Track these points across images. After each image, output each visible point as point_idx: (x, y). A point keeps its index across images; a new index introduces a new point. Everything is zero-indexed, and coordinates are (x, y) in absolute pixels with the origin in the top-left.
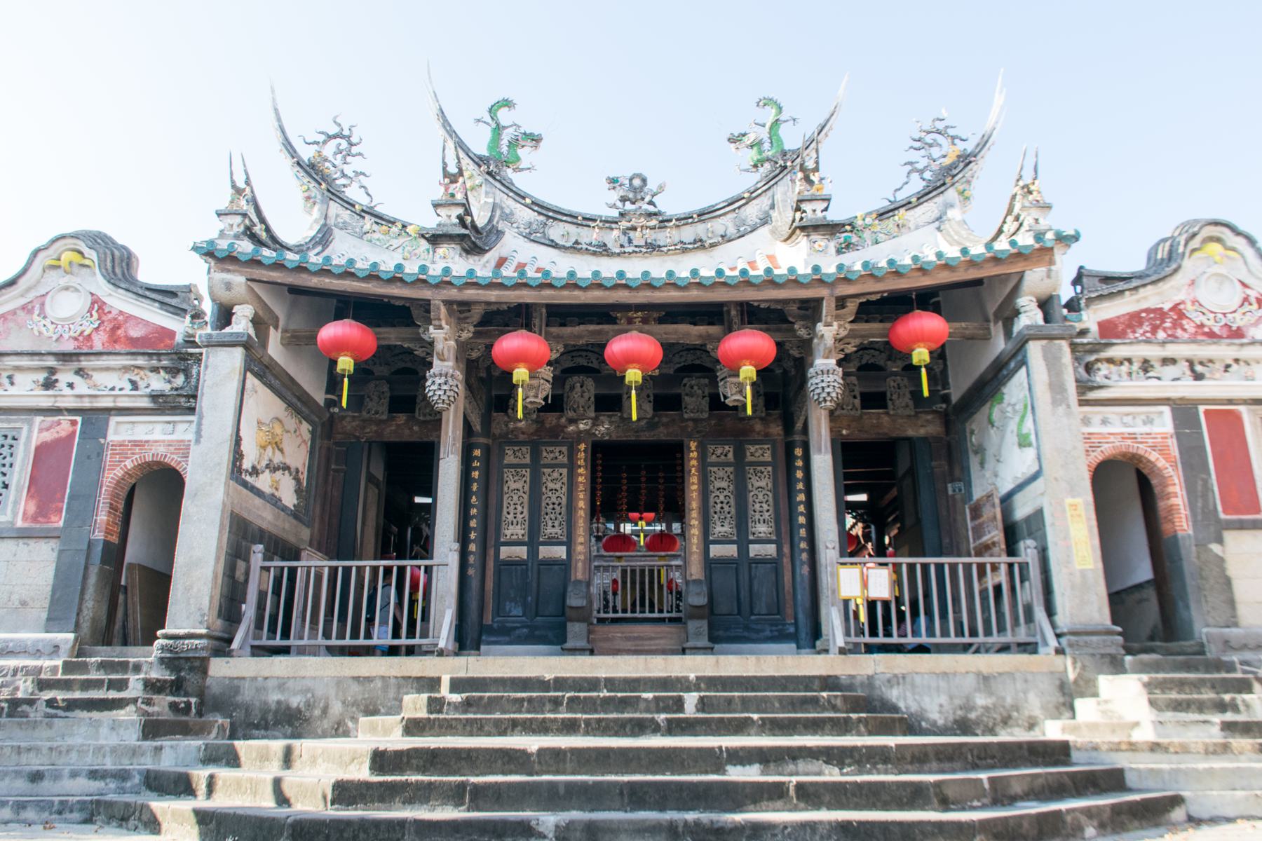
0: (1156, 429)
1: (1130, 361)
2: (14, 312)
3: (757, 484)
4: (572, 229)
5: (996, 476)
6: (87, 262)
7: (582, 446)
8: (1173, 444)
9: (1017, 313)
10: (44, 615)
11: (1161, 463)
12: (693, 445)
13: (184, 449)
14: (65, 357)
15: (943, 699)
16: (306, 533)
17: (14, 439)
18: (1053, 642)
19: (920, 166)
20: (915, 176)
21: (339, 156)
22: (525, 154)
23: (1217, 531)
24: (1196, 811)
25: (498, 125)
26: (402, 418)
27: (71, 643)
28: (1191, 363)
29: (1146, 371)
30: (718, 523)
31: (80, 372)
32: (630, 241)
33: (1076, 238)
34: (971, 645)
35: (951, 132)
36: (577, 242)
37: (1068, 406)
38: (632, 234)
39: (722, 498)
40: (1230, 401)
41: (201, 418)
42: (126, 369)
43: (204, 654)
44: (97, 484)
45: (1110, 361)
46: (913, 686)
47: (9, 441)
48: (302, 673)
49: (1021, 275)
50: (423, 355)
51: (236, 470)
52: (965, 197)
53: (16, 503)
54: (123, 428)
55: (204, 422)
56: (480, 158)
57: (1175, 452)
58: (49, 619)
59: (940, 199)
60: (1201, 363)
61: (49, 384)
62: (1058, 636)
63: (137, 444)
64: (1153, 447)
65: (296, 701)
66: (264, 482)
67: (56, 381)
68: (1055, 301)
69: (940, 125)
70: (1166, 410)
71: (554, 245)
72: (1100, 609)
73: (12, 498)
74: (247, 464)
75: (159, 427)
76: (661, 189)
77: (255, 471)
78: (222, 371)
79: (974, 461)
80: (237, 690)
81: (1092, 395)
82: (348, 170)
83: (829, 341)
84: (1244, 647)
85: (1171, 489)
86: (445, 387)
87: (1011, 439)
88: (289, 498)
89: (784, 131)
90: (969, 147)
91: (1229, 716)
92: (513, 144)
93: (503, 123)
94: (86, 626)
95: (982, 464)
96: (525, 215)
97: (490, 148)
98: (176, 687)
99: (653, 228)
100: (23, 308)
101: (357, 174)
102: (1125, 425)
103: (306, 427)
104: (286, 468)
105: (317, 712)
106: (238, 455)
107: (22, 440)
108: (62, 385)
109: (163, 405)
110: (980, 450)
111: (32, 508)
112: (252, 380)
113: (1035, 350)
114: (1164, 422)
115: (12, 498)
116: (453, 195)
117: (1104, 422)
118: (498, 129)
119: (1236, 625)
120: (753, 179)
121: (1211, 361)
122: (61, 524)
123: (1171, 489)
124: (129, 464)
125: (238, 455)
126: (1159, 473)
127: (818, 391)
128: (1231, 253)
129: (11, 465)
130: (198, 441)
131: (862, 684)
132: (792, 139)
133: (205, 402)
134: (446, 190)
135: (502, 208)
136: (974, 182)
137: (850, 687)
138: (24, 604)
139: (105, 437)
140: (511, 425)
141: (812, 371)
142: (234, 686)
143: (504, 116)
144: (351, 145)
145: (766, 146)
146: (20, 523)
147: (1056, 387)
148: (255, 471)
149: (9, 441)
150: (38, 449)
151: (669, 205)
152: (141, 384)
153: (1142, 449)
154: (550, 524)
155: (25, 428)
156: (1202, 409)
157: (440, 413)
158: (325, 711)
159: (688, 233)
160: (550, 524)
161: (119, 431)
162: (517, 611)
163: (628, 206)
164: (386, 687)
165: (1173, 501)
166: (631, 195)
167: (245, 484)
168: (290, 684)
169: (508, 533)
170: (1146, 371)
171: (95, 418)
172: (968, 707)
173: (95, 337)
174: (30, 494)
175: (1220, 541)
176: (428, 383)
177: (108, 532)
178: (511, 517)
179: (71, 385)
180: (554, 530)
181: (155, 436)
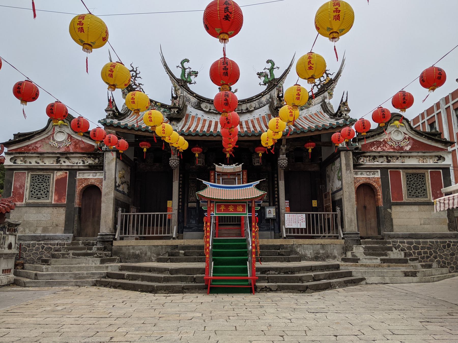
0: (376, 176)
2: (44, 139)
3: (264, 185)
4: (209, 105)
6: (66, 124)
8: (380, 180)
10: (63, 229)
11: (376, 186)
13: (101, 181)
14: (62, 154)
15: (311, 251)
16: (130, 200)
18: (342, 236)
19: (317, 84)
20: (315, 87)
21: (133, 78)
22: (192, 78)
23: (391, 205)
24: (368, 281)
25: (184, 67)
26: (158, 164)
27: (72, 237)
28: (387, 157)
31: (67, 158)
34: (320, 236)
35: (327, 72)
36: (210, 110)
40: (397, 168)
41: (105, 173)
42: (80, 157)
43: (112, 240)
44: (74, 191)
45: (365, 156)
46: (304, 248)
47: (47, 178)
48: (139, 244)
51: (116, 186)
52: (331, 95)
53: (52, 197)
54: (81, 175)
56: (178, 79)
57: (380, 183)
58: (65, 230)
59: (322, 95)
60: (390, 157)
61: (58, 162)
62: (343, 234)
63: (85, 179)
64: (374, 182)
65: (138, 252)
66: (120, 189)
67: (60, 160)
70: (379, 171)
71: (202, 110)
72: (355, 227)
74: (117, 184)
75: (91, 174)
77: (119, 186)
78: (110, 159)
79: (327, 179)
80: (121, 249)
82: (137, 82)
83: (284, 151)
84: (394, 237)
85: (378, 193)
87: (336, 176)
88: (126, 191)
89: (275, 72)
90: (332, 77)
91: (382, 257)
92: (190, 74)
93: (186, 67)
94: (75, 232)
96: (194, 100)
97: (181, 76)
98: (105, 249)
100: (47, 137)
101: (140, 84)
102: (367, 175)
103: (129, 168)
104: (125, 182)
105: (143, 255)
106: (116, 182)
107: (52, 178)
108: (62, 162)
109: (91, 168)
110: (329, 177)
111: (56, 198)
112: (118, 159)
113: (343, 154)
114: (378, 175)
115: (50, 195)
116: (175, 104)
117: (361, 174)
118: (184, 69)
119: (393, 231)
120: (264, 88)
122: (66, 202)
123: (378, 193)
124: (84, 185)
125: (116, 182)
128: (402, 124)
130: (105, 180)
131: (290, 247)
132: (277, 74)
134: (173, 102)
135: (186, 97)
136: (334, 90)
137: (287, 248)
138: (57, 225)
139: (76, 177)
140: (191, 167)
142: (120, 248)
143: (186, 65)
144: (137, 74)
145: (269, 77)
146: (53, 202)
147: (347, 165)
148: (119, 186)
149: (47, 178)
150: (56, 181)
152: (86, 162)
155: (52, 175)
156: (389, 170)
157: (173, 170)
158: (146, 254)
161: (80, 176)
162: (194, 222)
164: (162, 248)
165: (379, 197)
167: (117, 190)
168: (136, 247)
169: (191, 199)
171: (73, 171)
172: (318, 253)
173: (70, 147)
174: (55, 194)
175: (391, 208)
176: (170, 162)
177: (79, 205)
178: (191, 194)
179: (64, 162)
181: (91, 177)
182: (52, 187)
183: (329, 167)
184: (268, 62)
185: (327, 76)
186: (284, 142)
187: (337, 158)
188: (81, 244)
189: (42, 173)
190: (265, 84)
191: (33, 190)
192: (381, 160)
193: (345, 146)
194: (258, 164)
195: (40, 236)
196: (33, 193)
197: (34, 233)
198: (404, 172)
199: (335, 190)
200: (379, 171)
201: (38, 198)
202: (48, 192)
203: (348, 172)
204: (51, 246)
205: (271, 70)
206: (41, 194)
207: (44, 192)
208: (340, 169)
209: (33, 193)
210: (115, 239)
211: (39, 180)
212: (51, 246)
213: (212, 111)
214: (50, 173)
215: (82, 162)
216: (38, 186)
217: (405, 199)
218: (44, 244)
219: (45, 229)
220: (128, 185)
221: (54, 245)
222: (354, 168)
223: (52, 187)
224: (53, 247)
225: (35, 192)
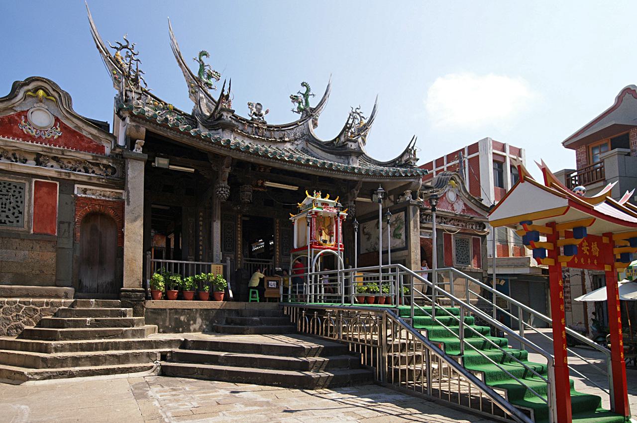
12: (278, 221)
17: (20, 188)
35: (361, 115)
50: (203, 174)
69: (358, 111)
73: (26, 219)
76: (267, 112)
89: (310, 98)
115: (26, 219)
120: (298, 117)
129: (22, 202)
132: (313, 104)
151: (271, 120)
154: (228, 245)
159: (277, 135)
160: (228, 245)
163: (254, 117)
182: (29, 206)
184: (303, 84)
185: (361, 120)
189: (6, 179)
190: (298, 112)
202: (20, 213)
205: (306, 95)
206: (7, 217)
207: (13, 214)
210: (147, 298)
214: (23, 181)
215: (83, 170)
218: (20, 302)
223: (29, 206)
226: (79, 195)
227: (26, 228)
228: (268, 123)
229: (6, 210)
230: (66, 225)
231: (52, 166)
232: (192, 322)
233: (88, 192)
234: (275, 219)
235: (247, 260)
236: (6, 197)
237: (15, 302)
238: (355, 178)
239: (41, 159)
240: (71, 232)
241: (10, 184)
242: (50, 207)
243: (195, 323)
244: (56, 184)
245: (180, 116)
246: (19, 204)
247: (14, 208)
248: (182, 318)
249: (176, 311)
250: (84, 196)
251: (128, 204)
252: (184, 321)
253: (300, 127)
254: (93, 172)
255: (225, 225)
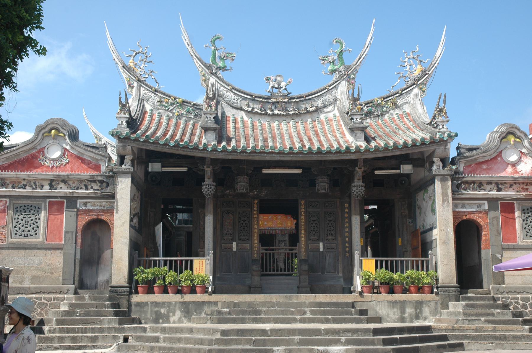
1: (474, 183)
5: (424, 221)
7: (256, 202)
9: (433, 162)
10: (61, 278)
11: (482, 223)
12: (303, 202)
17: (39, 208)
22: (228, 63)
27: (74, 289)
29: (480, 187)
30: (312, 235)
32: (276, 107)
33: (456, 135)
36: (253, 109)
37: (448, 202)
38: (276, 104)
39: (314, 225)
41: (117, 202)
43: (128, 294)
49: (435, 150)
55: (119, 204)
58: (63, 280)
60: (501, 184)
68: (447, 160)
70: (486, 202)
79: (418, 212)
81: (458, 196)
86: (210, 190)
87: (429, 209)
88: (137, 225)
95: (420, 213)
99: (286, 102)
110: (420, 208)
117: (463, 206)
121: (505, 183)
122: (63, 242)
126: (481, 226)
127: (355, 193)
128: (518, 140)
129: (39, 219)
133: (118, 196)
141: (353, 184)
147: (444, 195)
152: (89, 187)
153: (474, 217)
154: (242, 234)
160: (242, 234)
163: (275, 91)
166: (276, 86)
170: (480, 187)
176: (204, 187)
180: (244, 237)
183: (421, 194)
186: (360, 164)
187: (432, 184)
188: (87, 298)
189: (29, 202)
191: (18, 226)
192: (488, 187)
193: (441, 168)
194: (324, 191)
195: (29, 288)
196: (17, 229)
197: (20, 283)
198: (519, 204)
199: (428, 227)
200: (486, 202)
201: (25, 236)
202: (38, 227)
203: (445, 204)
204: (45, 302)
206: (29, 231)
207: (33, 229)
208: (434, 202)
209: (17, 229)
211: (25, 212)
212: (45, 302)
213: (256, 110)
215: (84, 187)
216: (24, 219)
217: (521, 241)
219: (35, 278)
220: (138, 217)
221: (49, 300)
222: (453, 199)
224: (48, 303)
225: (20, 228)
226: (81, 208)
227: (41, 239)
228: (293, 94)
229: (28, 226)
230: (70, 234)
231: (61, 188)
232: (171, 314)
233: (88, 205)
234: (300, 200)
235: (266, 250)
236: (29, 216)
237: (32, 298)
238: (353, 157)
239: (53, 184)
240: (74, 239)
241: (31, 206)
242: (59, 220)
243: (174, 315)
244: (63, 202)
245: (191, 107)
246: (37, 221)
247: (34, 224)
248: (162, 311)
249: (156, 304)
250: (84, 208)
251: (117, 212)
252: (164, 313)
253: (331, 91)
254: (92, 188)
255: (240, 213)
